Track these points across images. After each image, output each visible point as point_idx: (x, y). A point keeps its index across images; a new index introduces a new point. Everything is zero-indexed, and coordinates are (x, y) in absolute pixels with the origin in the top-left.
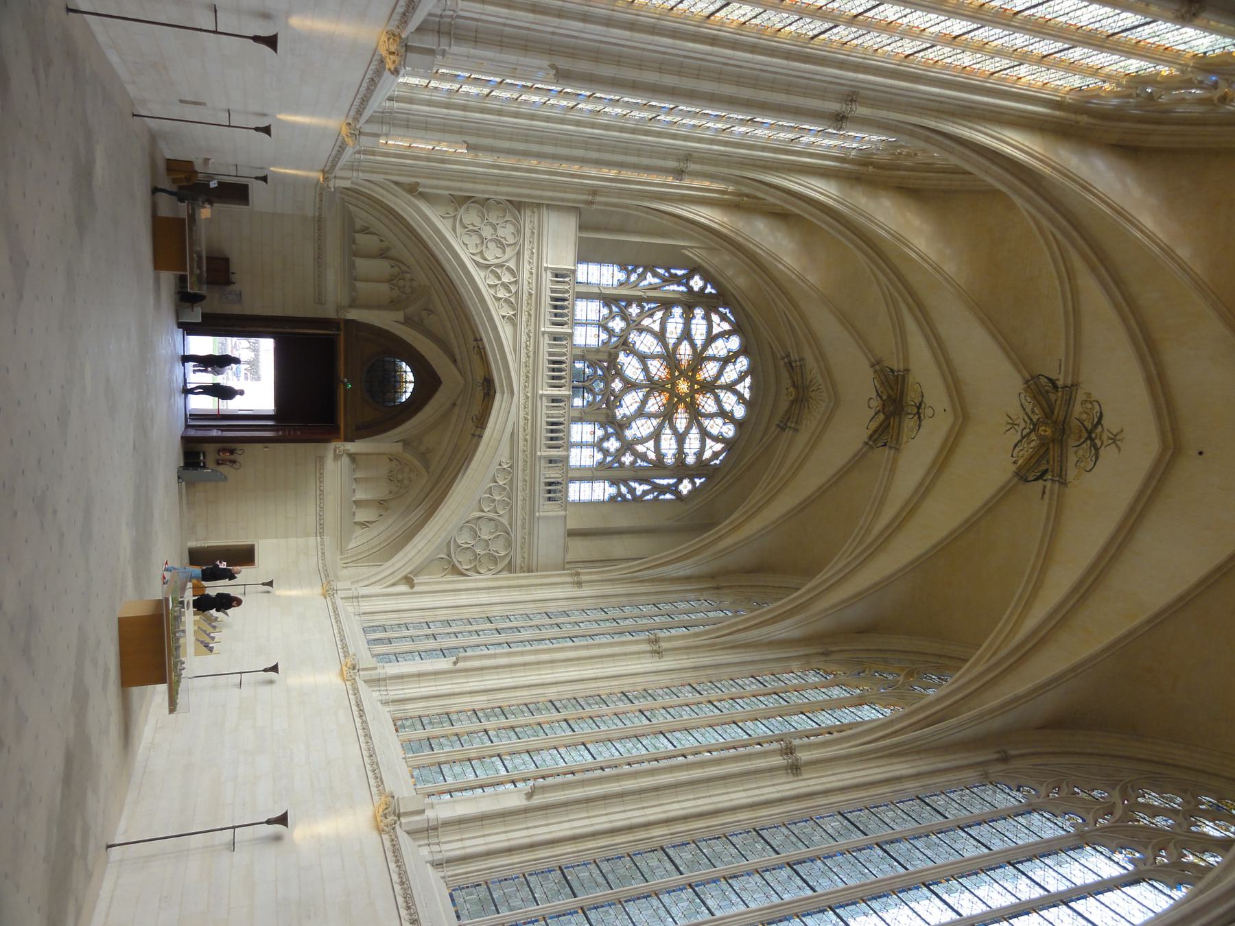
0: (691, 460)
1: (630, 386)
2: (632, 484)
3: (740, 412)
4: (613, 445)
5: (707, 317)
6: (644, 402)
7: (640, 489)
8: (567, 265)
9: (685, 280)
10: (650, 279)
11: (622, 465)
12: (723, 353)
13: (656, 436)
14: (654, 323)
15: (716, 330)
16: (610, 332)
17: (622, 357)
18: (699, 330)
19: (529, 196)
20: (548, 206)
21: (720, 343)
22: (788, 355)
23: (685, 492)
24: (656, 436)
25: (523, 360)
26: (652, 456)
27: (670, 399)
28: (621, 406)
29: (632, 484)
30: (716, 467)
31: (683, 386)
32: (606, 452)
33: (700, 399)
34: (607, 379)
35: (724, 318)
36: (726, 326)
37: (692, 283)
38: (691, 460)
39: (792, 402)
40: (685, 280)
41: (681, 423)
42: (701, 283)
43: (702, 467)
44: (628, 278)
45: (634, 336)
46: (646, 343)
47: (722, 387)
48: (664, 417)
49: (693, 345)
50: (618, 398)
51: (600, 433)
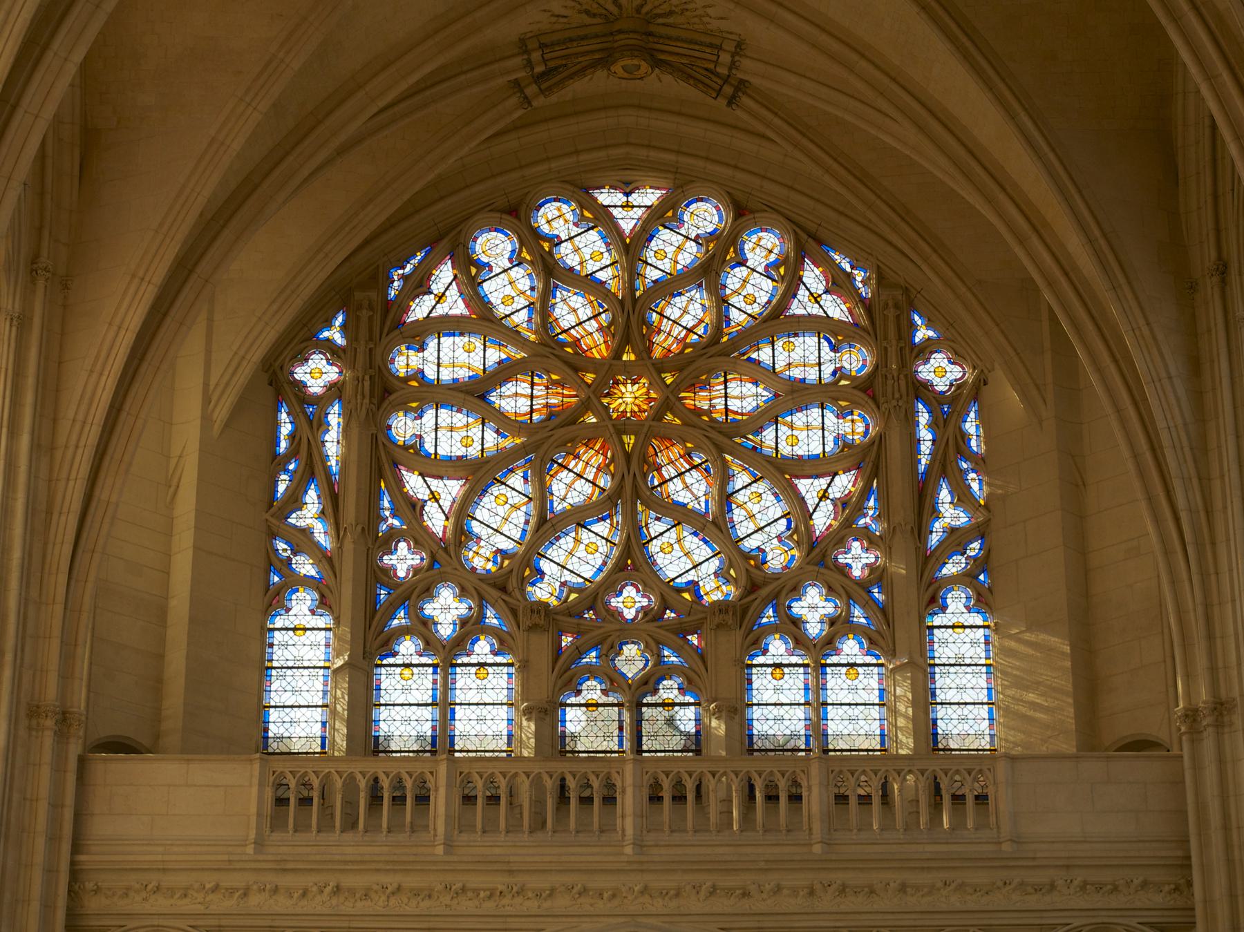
0: (856, 360)
1: (632, 561)
2: (934, 539)
3: (705, 216)
4: (813, 607)
5: (418, 336)
6: (679, 514)
7: (950, 514)
8: (237, 787)
9: (309, 411)
10: (309, 514)
11: (877, 575)
12: (523, 278)
13: (784, 472)
14: (438, 498)
15: (455, 305)
16: (470, 628)
17: (542, 592)
18: (457, 357)
19: (47, 906)
20: (76, 848)
21: (494, 290)
22: (517, 85)
23: (955, 372)
24: (784, 472)
25: (532, 905)
26: (844, 483)
27: (668, 438)
28: (693, 586)
29: (934, 539)
30: (881, 280)
31: (630, 397)
32: (839, 626)
33: (664, 343)
34: (615, 632)
35: (419, 285)
36: (445, 274)
37: (316, 387)
38: (856, 360)
39: (657, 63)
40: (309, 411)
41: (744, 397)
42: (317, 362)
43: (882, 323)
44: (307, 581)
45: (480, 560)
46: (501, 519)
47: (632, 274)
48: (721, 450)
49: (504, 373)
50: (668, 593)
51: (777, 648)
